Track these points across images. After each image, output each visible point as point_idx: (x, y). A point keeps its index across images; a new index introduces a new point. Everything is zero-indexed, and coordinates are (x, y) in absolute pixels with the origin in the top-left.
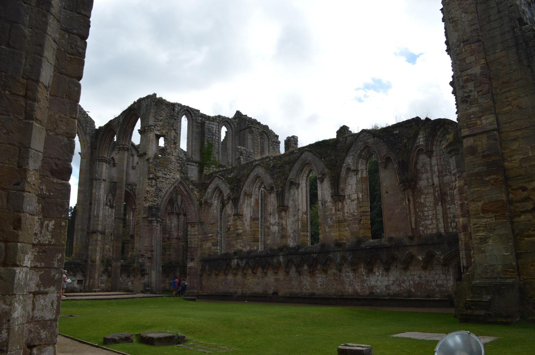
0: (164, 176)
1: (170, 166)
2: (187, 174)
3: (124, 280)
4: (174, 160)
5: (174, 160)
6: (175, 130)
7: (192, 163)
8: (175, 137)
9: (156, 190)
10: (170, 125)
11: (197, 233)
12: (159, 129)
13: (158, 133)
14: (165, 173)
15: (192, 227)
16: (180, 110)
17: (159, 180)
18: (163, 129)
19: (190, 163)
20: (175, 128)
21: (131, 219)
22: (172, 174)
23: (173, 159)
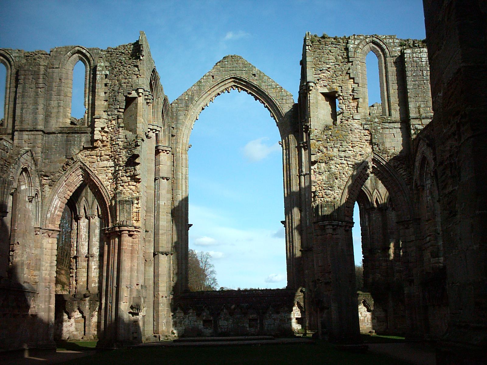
0: (342, 154)
1: (351, 137)
2: (383, 143)
3: (365, 317)
4: (356, 126)
5: (356, 126)
6: (353, 78)
7: (392, 125)
8: (353, 90)
9: (328, 178)
10: (345, 72)
11: (413, 238)
12: (326, 84)
13: (326, 90)
14: (343, 149)
15: (407, 228)
16: (358, 44)
17: (332, 162)
18: (333, 83)
19: (387, 125)
20: (352, 76)
21: (367, 224)
22: (357, 149)
23: (356, 124)
